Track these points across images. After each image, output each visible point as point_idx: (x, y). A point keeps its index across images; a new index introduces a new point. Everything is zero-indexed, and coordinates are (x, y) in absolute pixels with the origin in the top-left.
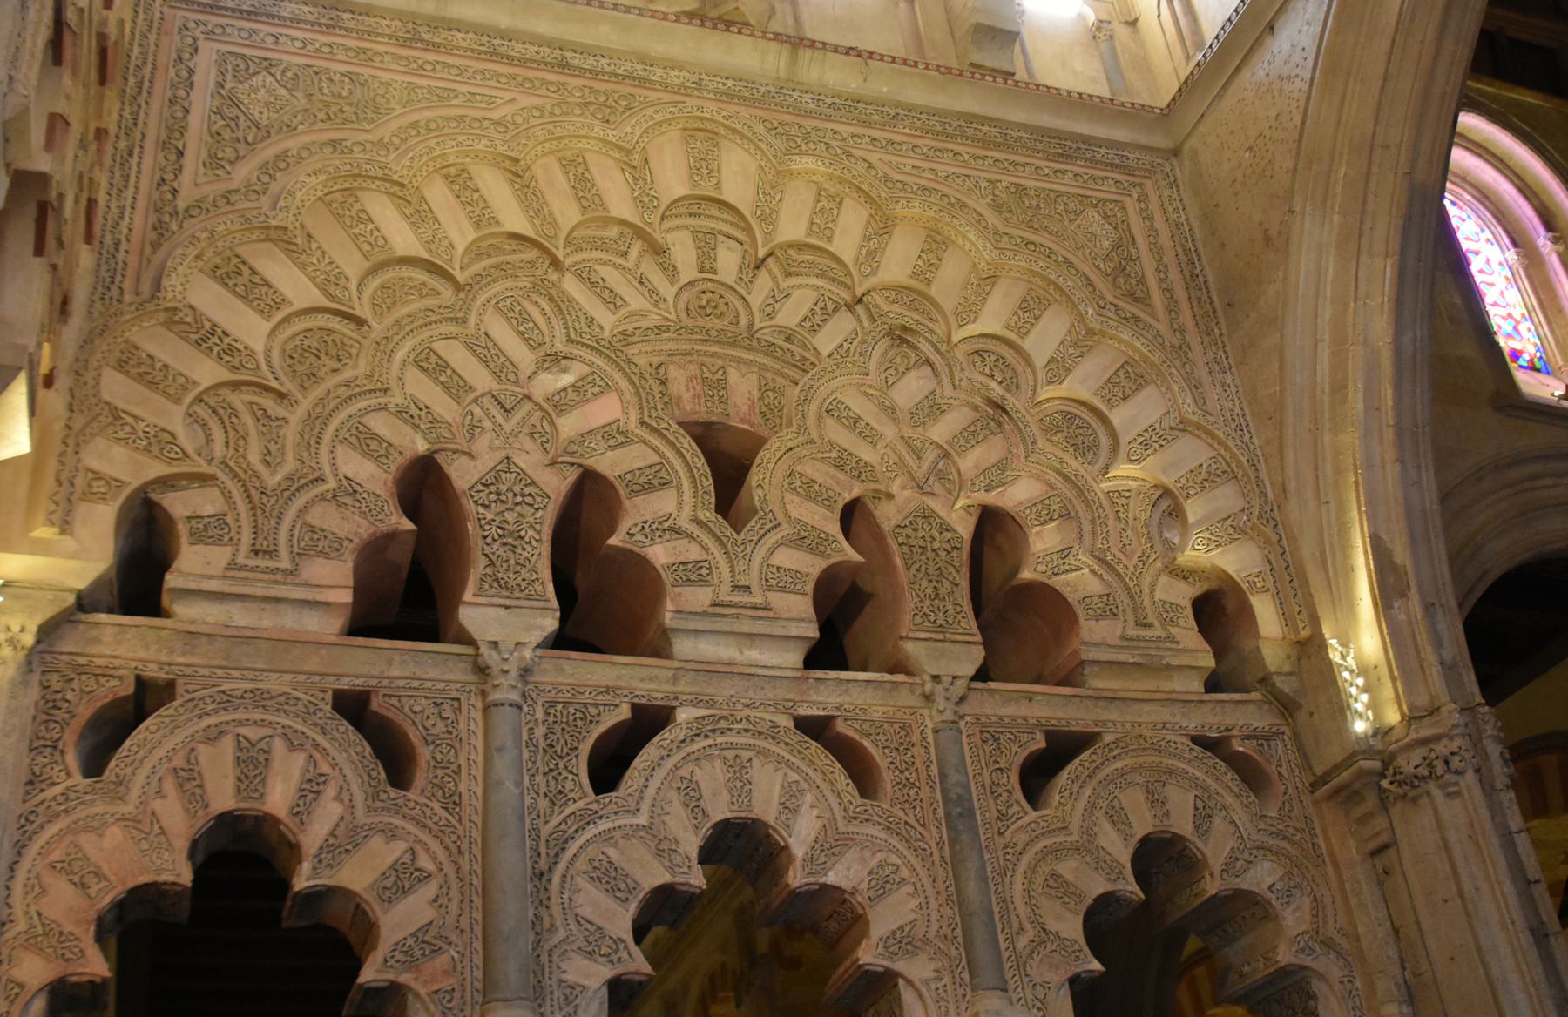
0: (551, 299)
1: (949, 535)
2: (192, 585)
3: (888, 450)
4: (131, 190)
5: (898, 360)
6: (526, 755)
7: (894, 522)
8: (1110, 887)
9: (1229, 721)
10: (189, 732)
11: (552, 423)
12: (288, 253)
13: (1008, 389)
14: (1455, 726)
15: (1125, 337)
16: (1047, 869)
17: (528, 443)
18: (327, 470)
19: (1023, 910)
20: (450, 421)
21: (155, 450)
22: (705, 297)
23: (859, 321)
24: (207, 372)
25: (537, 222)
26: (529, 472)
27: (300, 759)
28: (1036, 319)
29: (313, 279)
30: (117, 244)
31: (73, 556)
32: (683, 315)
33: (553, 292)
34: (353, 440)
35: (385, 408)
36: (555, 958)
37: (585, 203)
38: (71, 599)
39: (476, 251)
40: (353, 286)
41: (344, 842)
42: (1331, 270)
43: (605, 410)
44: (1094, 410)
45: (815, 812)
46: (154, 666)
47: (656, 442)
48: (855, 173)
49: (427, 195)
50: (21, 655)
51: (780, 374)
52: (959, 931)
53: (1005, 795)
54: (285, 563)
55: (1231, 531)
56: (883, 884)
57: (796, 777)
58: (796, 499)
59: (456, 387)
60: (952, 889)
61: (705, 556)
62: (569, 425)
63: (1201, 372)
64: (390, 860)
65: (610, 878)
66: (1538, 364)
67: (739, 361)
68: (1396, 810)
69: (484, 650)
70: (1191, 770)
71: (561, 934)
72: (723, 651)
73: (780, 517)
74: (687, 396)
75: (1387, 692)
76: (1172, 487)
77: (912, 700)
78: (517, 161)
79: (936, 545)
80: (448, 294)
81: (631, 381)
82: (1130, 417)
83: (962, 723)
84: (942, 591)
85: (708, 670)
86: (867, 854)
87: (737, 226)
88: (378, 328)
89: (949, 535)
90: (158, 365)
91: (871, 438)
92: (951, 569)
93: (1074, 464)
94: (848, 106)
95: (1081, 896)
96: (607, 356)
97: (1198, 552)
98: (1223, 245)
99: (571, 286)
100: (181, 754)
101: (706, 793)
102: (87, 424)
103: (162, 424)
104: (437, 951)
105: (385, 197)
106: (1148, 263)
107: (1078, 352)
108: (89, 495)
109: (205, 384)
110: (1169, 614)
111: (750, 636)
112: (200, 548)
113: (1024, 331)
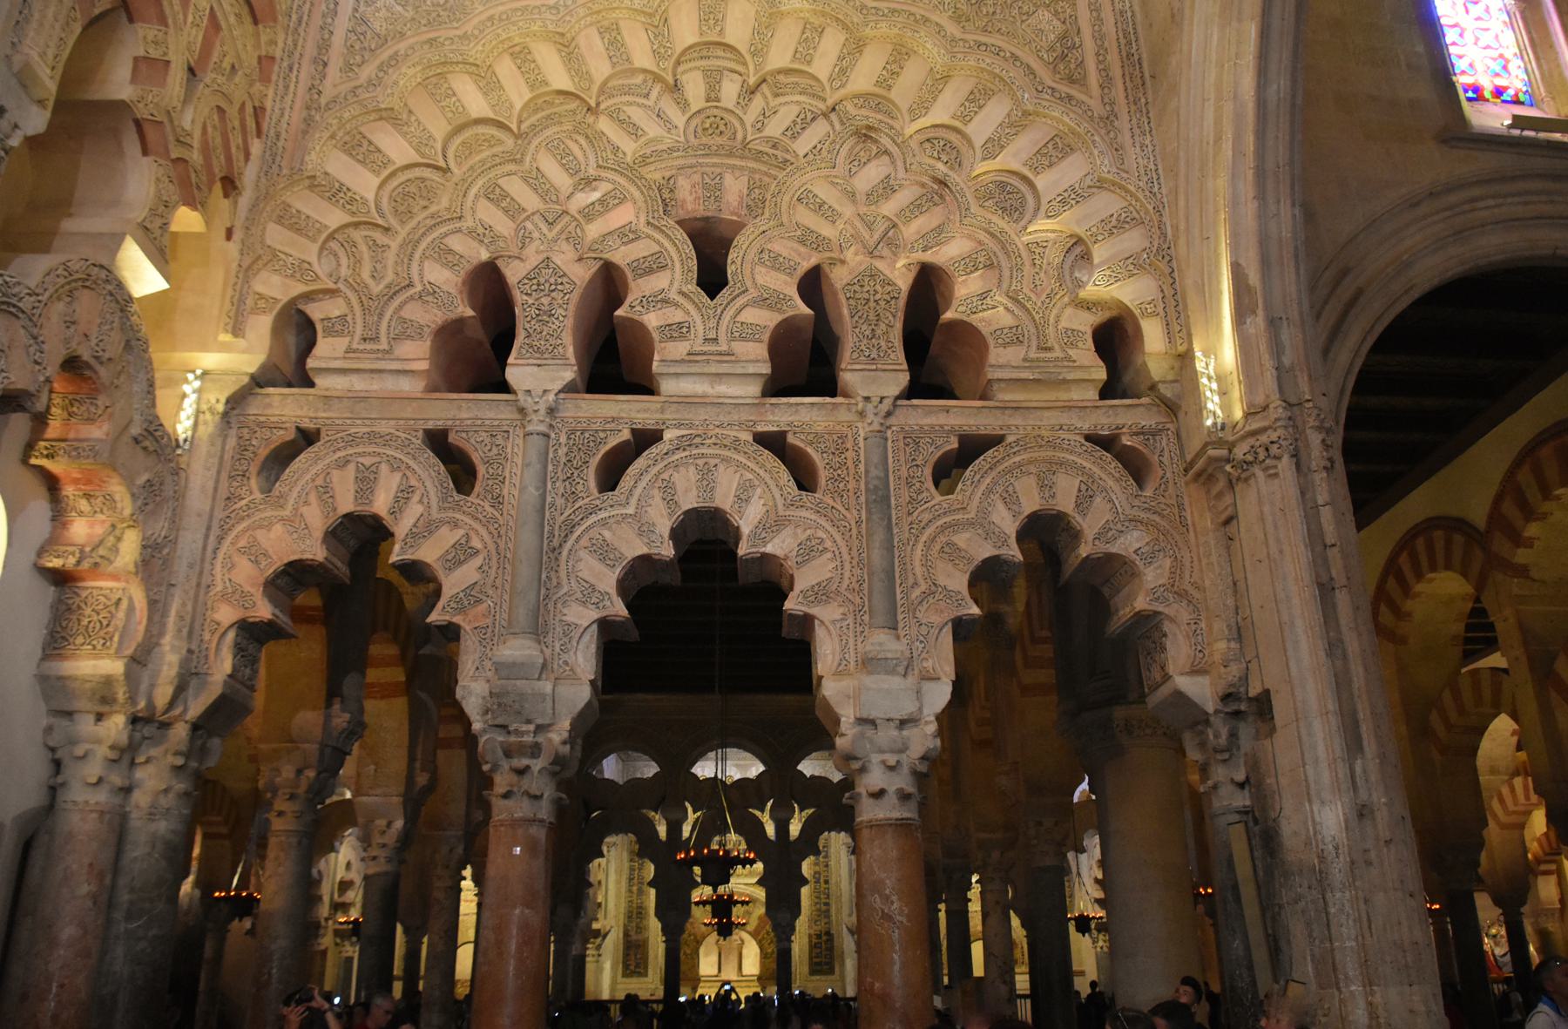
0: (587, 137)
1: (890, 288)
2: (324, 365)
3: (848, 226)
4: (291, 96)
5: (862, 153)
6: (550, 468)
7: (845, 282)
8: (996, 552)
9: (1120, 421)
10: (326, 462)
11: (582, 230)
12: (395, 126)
13: (952, 168)
14: (1277, 420)
15: (1056, 114)
16: (944, 540)
17: (565, 246)
18: (416, 278)
19: (919, 570)
20: (506, 234)
21: (298, 275)
22: (708, 121)
23: (832, 125)
24: (334, 218)
25: (576, 80)
26: (563, 267)
27: (397, 477)
28: (980, 107)
29: (410, 143)
30: (278, 136)
31: (244, 352)
32: (691, 138)
33: (589, 132)
34: (436, 255)
35: (459, 231)
36: (559, 605)
37: (614, 60)
38: (246, 380)
39: (531, 106)
40: (439, 146)
41: (425, 529)
42: (1215, 37)
43: (622, 216)
44: (1024, 178)
45: (762, 502)
46: (306, 420)
47: (657, 236)
48: (834, 6)
49: (498, 70)
50: (217, 418)
51: (766, 174)
52: (865, 585)
53: (918, 485)
54: (384, 345)
55: (1131, 267)
56: (809, 551)
57: (751, 476)
58: (763, 270)
59: (513, 211)
60: (864, 555)
61: (687, 318)
62: (593, 230)
63: (1126, 138)
64: (452, 542)
65: (604, 552)
66: (1522, 97)
67: (734, 167)
68: (1239, 488)
69: (521, 396)
70: (1079, 461)
71: (565, 590)
73: (749, 284)
74: (690, 199)
75: (1236, 393)
76: (1083, 235)
77: (851, 417)
78: (563, 35)
79: (878, 297)
80: (509, 142)
81: (642, 193)
83: (889, 432)
84: (879, 332)
85: (687, 401)
86: (799, 531)
87: (738, 62)
88: (455, 170)
89: (890, 288)
90: (303, 217)
91: (832, 216)
92: (888, 314)
93: (1000, 223)
95: (970, 560)
96: (625, 176)
98: (1151, 25)
99: (604, 124)
100: (322, 476)
101: (679, 493)
102: (254, 262)
103: (303, 257)
104: (479, 601)
105: (467, 78)
106: (1089, 46)
107: (1013, 131)
108: (256, 310)
109: (334, 226)
110: (1071, 337)
111: (718, 374)
112: (330, 339)
113: (968, 118)
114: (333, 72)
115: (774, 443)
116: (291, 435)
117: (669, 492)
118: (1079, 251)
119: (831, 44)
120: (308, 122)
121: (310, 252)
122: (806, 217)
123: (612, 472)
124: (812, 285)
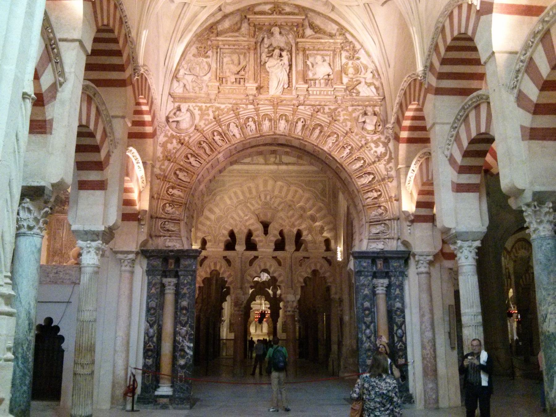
24: (208, 223)
39: (238, 202)
59: (235, 220)
72: (264, 250)
80: (234, 208)
85: (263, 252)
93: (311, 222)
97: (326, 234)
99: (249, 205)
110: (320, 242)
115: (275, 258)
116: (203, 257)
117: (260, 266)
119: (285, 189)
120: (203, 206)
121: (205, 229)
122: (281, 221)
123: (251, 263)
124: (281, 233)
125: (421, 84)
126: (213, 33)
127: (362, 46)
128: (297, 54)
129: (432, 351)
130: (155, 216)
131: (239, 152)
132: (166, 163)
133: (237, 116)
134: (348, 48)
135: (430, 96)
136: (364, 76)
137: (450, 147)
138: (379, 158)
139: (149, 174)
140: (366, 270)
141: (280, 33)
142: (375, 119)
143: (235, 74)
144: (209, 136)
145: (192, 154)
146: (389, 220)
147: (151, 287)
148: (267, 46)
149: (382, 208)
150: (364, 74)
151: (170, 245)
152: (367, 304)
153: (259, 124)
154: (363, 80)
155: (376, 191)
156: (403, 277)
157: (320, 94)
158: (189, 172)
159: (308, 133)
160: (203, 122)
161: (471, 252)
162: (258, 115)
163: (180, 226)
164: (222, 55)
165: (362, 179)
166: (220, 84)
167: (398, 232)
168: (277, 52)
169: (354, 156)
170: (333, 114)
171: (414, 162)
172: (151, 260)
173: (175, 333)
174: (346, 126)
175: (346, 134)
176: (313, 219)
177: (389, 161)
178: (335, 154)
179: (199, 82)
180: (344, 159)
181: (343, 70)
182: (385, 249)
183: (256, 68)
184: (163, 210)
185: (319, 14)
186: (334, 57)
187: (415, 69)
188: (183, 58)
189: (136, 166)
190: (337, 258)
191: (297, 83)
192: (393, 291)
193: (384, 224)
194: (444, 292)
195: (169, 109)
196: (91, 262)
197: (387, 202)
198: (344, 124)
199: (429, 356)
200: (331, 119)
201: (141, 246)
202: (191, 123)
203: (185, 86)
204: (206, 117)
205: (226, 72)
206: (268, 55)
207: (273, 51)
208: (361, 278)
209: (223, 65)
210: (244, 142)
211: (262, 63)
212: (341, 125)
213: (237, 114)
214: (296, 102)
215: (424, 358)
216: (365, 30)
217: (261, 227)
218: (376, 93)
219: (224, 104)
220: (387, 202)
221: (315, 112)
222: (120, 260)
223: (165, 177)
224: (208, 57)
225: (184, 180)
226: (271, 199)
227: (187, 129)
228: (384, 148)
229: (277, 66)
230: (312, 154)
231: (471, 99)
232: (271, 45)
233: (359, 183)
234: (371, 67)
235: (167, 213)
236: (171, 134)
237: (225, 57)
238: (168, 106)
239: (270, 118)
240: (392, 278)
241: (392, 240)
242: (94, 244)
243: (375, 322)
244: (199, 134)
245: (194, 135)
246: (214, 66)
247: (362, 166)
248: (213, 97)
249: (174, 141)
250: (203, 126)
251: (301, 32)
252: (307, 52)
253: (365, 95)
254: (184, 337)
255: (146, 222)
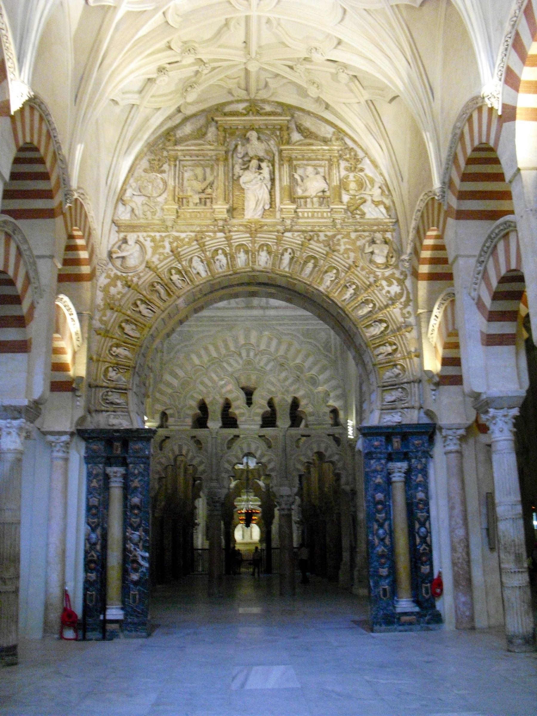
24: (170, 391)
39: (209, 361)
59: (206, 386)
62: (224, 391)
82: (321, 377)
85: (245, 429)
94: (275, 318)
97: (331, 403)
99: (225, 365)
110: (325, 414)
114: (165, 354)
116: (164, 438)
117: (242, 449)
118: (327, 394)
119: (274, 343)
120: (162, 367)
121: (166, 399)
122: (269, 386)
124: (270, 403)
125: (440, 204)
126: (169, 140)
127: (366, 154)
128: (281, 165)
129: (464, 554)
130: (95, 383)
131: (205, 295)
132: (109, 312)
133: (202, 247)
134: (348, 156)
135: (451, 221)
136: (371, 193)
137: (477, 286)
138: (393, 300)
139: (86, 328)
140: (378, 450)
141: (259, 138)
142: (386, 249)
143: (199, 193)
144: (165, 276)
145: (141, 300)
146: (407, 383)
147: (91, 479)
148: (240, 156)
149: (399, 367)
150: (370, 190)
151: (114, 423)
152: (380, 496)
153: (231, 258)
154: (369, 198)
155: (391, 344)
156: (427, 458)
157: (313, 216)
158: (138, 324)
159: (298, 268)
160: (157, 256)
161: (506, 423)
162: (230, 245)
163: (127, 397)
164: (181, 168)
165: (372, 329)
166: (179, 207)
167: (420, 398)
168: (254, 163)
169: (359, 299)
170: (331, 243)
171: (436, 306)
172: (90, 443)
173: (125, 539)
174: (349, 258)
175: (349, 268)
176: (313, 381)
177: (406, 305)
178: (335, 296)
179: (152, 204)
180: (346, 302)
181: (343, 185)
182: (404, 423)
183: (227, 184)
184: (105, 375)
185: (309, 113)
186: (330, 168)
187: (432, 185)
188: (130, 174)
189: (68, 318)
190: (347, 435)
191: (281, 202)
192: (414, 478)
193: (402, 388)
194: (481, 476)
195: (112, 242)
196: (12, 447)
197: (405, 359)
198: (346, 256)
199: (460, 561)
200: (327, 249)
201: (78, 424)
202: (141, 259)
203: (133, 210)
204: (161, 250)
205: (187, 190)
206: (243, 167)
207: (250, 161)
208: (372, 462)
209: (183, 180)
210: (211, 282)
211: (235, 178)
212: (341, 256)
213: (202, 245)
214: (280, 228)
215: (454, 564)
216: (369, 134)
217: (242, 395)
218: (386, 215)
219: (185, 232)
220: (405, 359)
221: (306, 241)
222: (50, 443)
223: (107, 331)
224: (163, 172)
225: (132, 335)
226: (256, 355)
227: (135, 267)
228: (400, 287)
229: (254, 182)
230: (304, 296)
231: (498, 227)
232: (247, 154)
233: (368, 335)
234: (379, 180)
235: (109, 380)
236: (115, 274)
237: (186, 171)
238: (112, 237)
239: (246, 249)
240: (413, 461)
241: (412, 410)
242: (16, 423)
243: (390, 519)
244: (151, 272)
245: (145, 275)
246: (171, 183)
247: (371, 311)
248: (170, 224)
249: (119, 283)
250: (157, 262)
251: (286, 137)
252: (295, 163)
253: (373, 217)
254: (136, 544)
255: (83, 390)
